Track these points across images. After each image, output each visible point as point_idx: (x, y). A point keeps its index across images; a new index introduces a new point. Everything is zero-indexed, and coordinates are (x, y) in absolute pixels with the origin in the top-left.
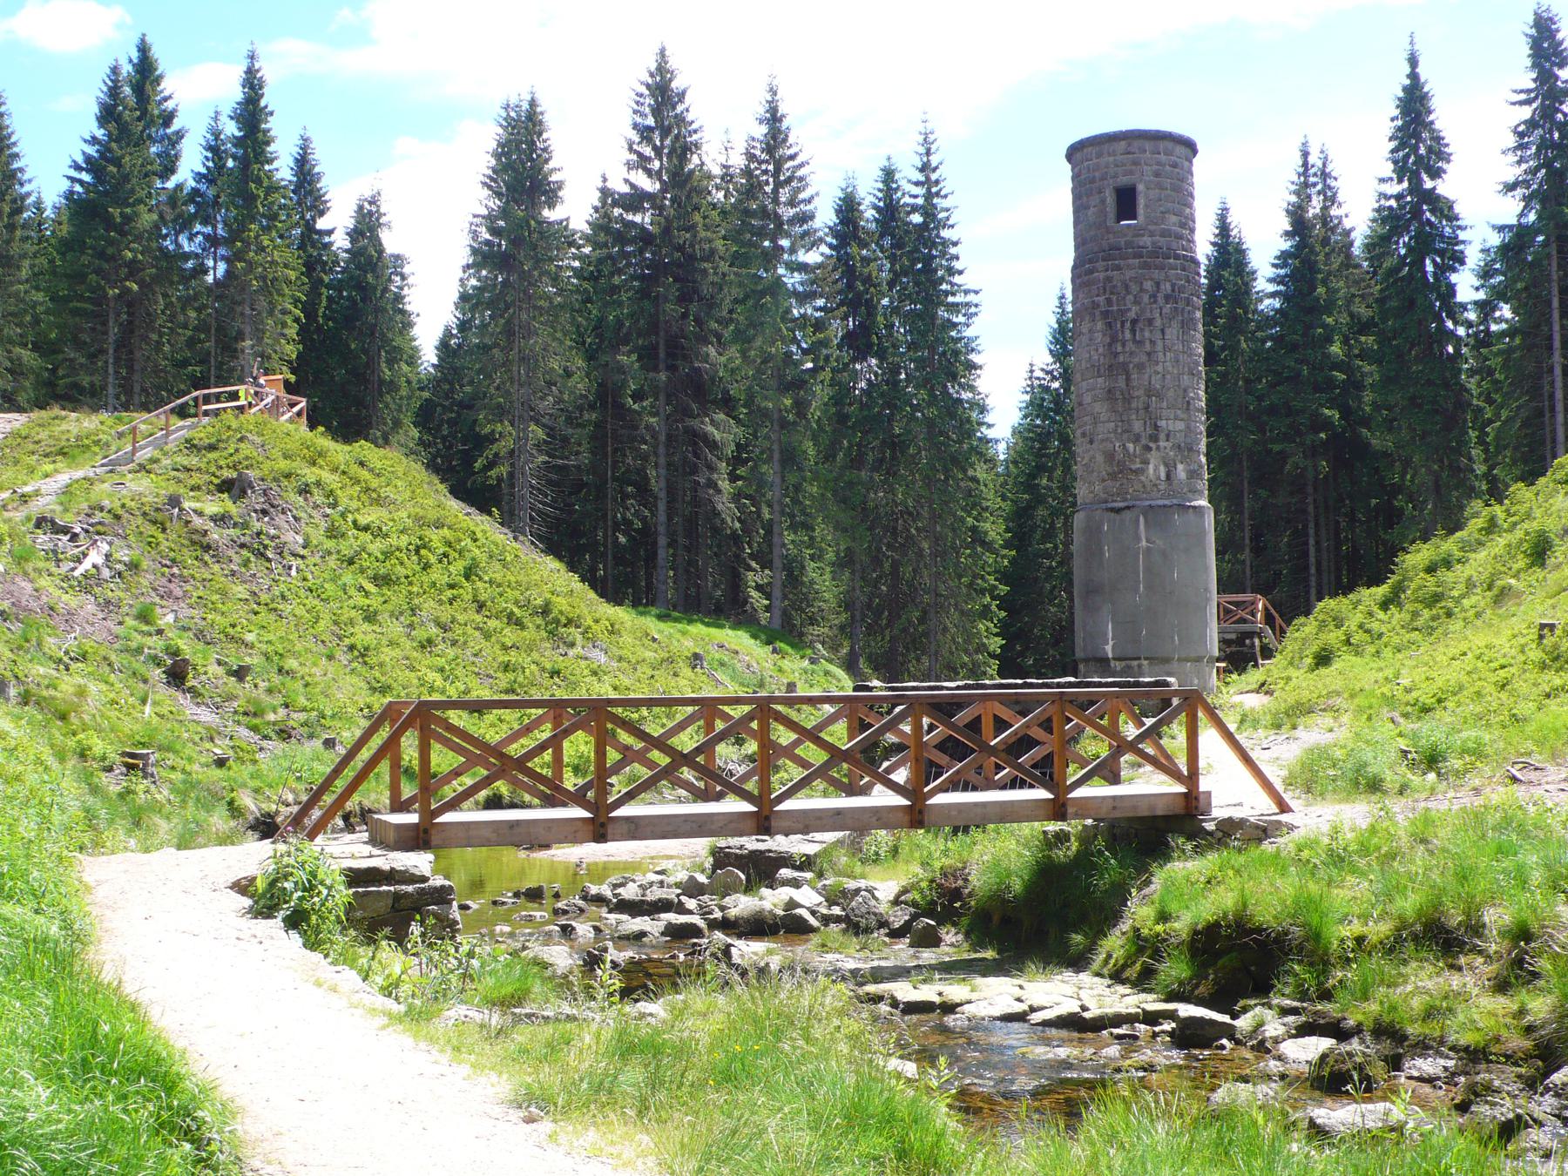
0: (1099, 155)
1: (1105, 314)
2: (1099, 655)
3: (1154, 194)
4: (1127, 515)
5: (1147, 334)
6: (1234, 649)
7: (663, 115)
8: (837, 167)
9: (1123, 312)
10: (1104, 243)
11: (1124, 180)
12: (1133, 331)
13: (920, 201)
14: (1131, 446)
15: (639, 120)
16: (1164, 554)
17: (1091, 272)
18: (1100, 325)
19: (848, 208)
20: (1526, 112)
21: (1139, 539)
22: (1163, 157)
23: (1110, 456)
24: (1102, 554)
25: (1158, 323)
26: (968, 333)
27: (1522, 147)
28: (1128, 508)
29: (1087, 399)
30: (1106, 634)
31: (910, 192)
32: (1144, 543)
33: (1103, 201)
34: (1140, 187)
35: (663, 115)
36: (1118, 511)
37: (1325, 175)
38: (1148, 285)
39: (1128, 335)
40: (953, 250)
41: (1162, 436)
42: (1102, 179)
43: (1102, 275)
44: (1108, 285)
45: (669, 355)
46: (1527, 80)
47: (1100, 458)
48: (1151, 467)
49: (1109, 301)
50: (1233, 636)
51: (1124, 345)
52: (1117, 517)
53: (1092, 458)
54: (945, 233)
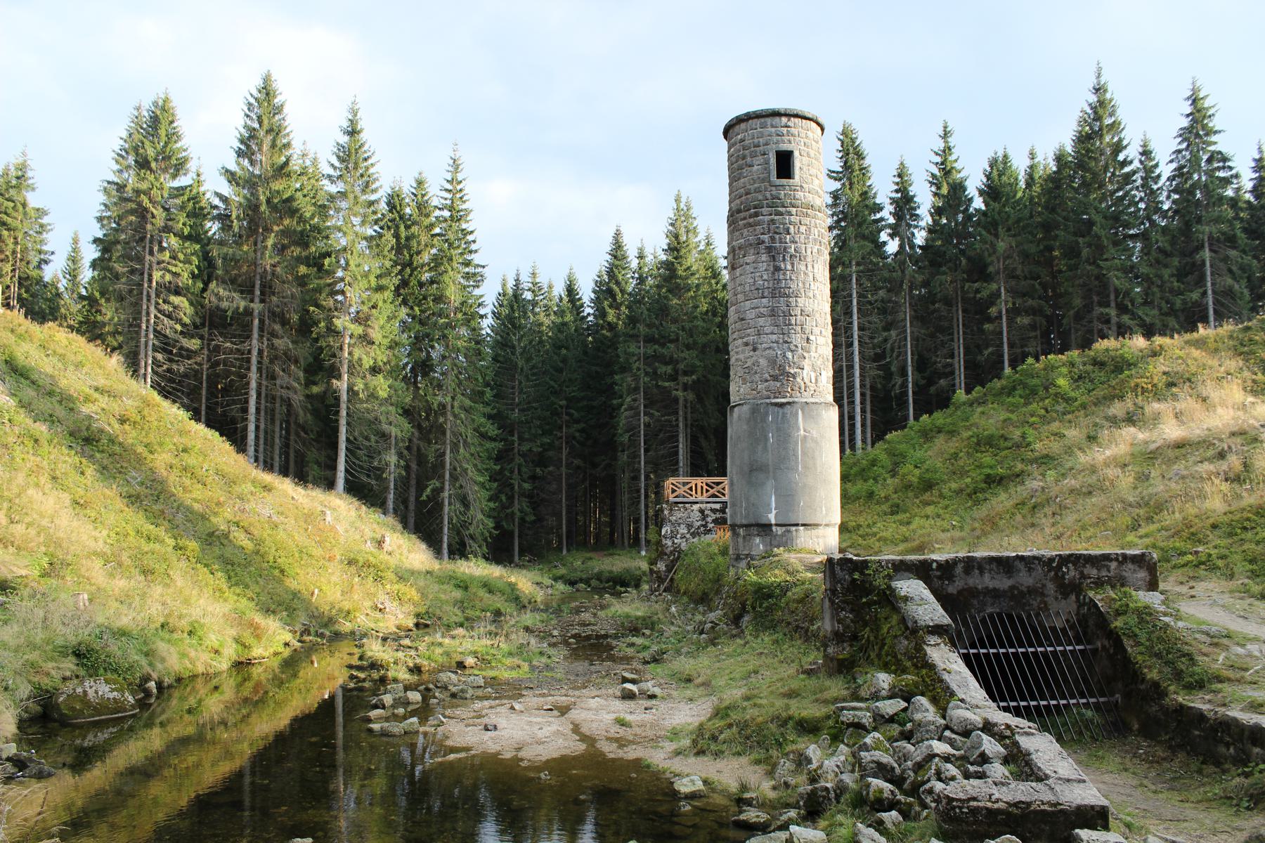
0: (764, 126)
1: (769, 249)
2: (764, 521)
3: (805, 159)
4: (788, 409)
5: (803, 268)
6: (718, 515)
7: (264, 125)
8: (392, 172)
9: (785, 248)
10: (768, 195)
11: (785, 147)
12: (793, 265)
13: (449, 202)
14: (789, 355)
15: (249, 122)
16: (816, 442)
17: (756, 215)
18: (764, 257)
19: (394, 202)
20: (837, 185)
21: (798, 429)
22: (810, 133)
23: (773, 362)
24: (767, 439)
25: (809, 259)
26: (477, 292)
27: (834, 205)
28: (789, 403)
29: (750, 315)
30: (769, 505)
31: (436, 195)
32: (802, 432)
33: (767, 162)
34: (796, 154)
35: (264, 125)
36: (782, 405)
37: (688, 217)
38: (803, 229)
39: (789, 267)
40: (470, 238)
41: (813, 348)
42: (767, 144)
43: (767, 218)
44: (772, 227)
45: (262, 293)
46: (837, 166)
47: (763, 362)
48: (805, 372)
49: (773, 239)
50: (718, 506)
51: (784, 274)
52: (781, 411)
53: (756, 363)
54: (464, 226)
